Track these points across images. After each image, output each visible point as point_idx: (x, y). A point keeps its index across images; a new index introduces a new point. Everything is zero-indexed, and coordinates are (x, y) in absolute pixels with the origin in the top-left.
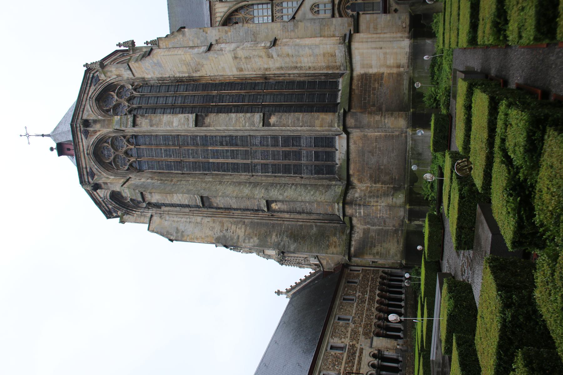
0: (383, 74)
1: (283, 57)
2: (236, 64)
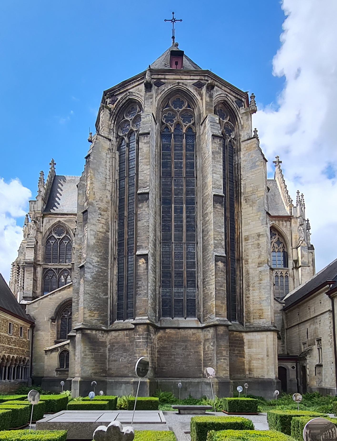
0: (244, 358)
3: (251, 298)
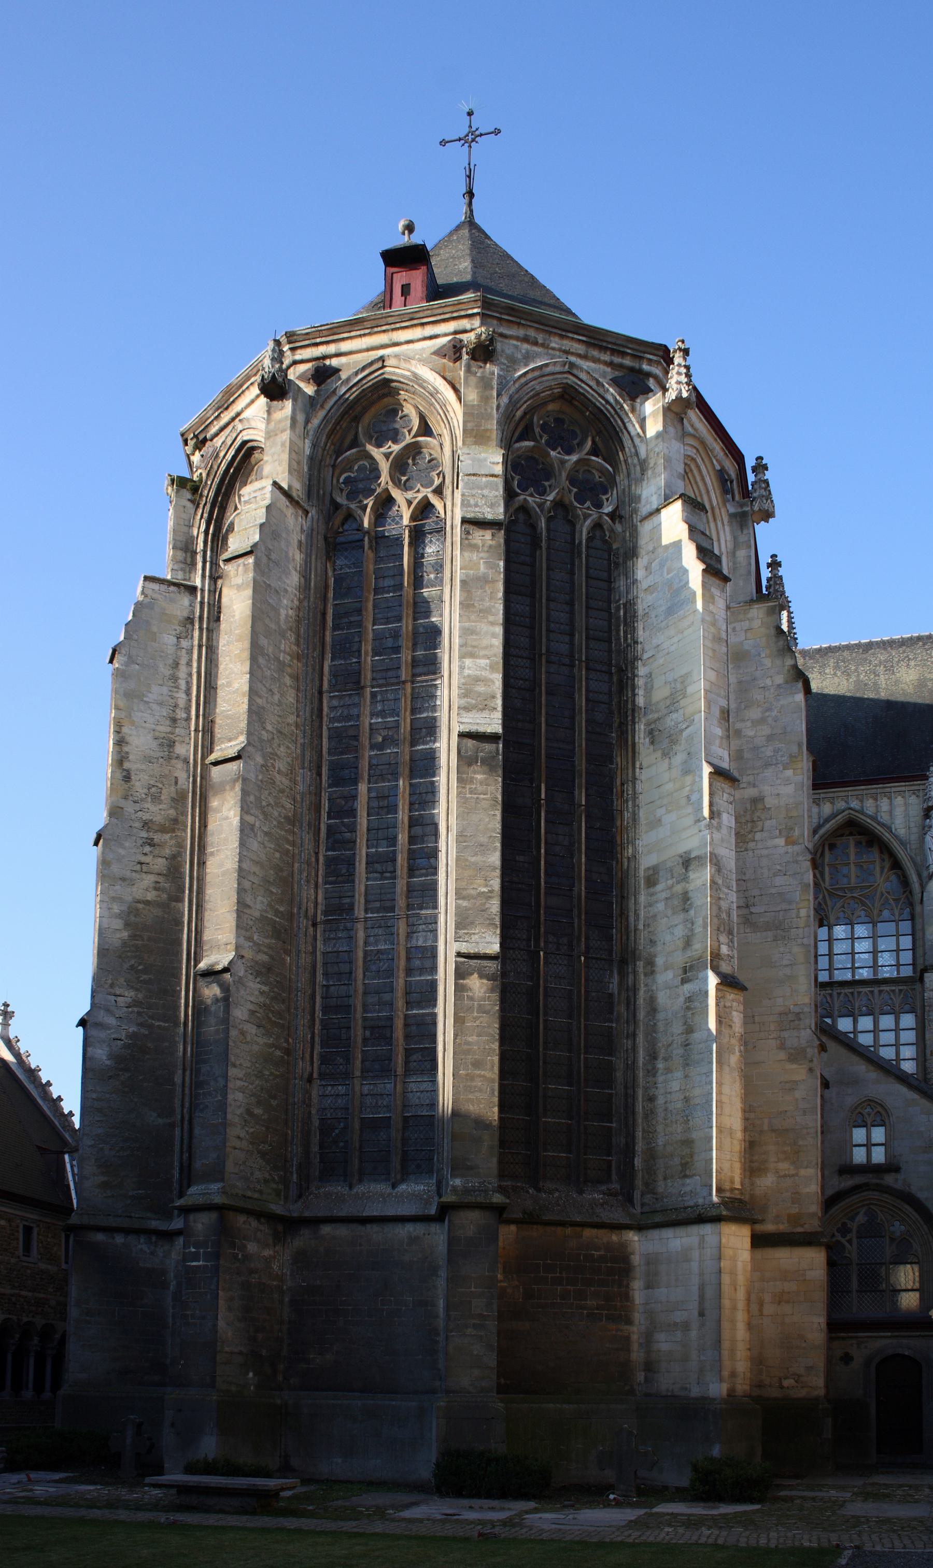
0: (629, 1322)
1: (684, 1016)
2: (669, 864)
3: (661, 1100)
